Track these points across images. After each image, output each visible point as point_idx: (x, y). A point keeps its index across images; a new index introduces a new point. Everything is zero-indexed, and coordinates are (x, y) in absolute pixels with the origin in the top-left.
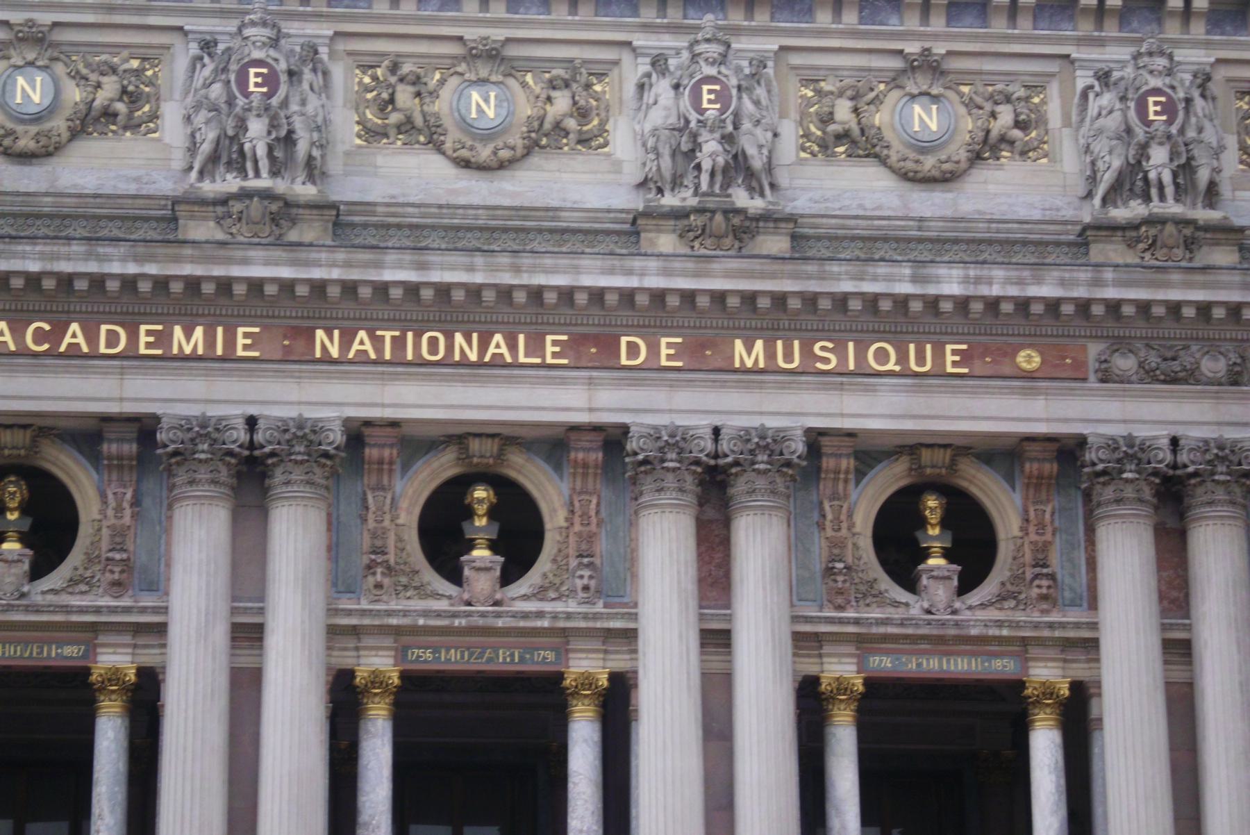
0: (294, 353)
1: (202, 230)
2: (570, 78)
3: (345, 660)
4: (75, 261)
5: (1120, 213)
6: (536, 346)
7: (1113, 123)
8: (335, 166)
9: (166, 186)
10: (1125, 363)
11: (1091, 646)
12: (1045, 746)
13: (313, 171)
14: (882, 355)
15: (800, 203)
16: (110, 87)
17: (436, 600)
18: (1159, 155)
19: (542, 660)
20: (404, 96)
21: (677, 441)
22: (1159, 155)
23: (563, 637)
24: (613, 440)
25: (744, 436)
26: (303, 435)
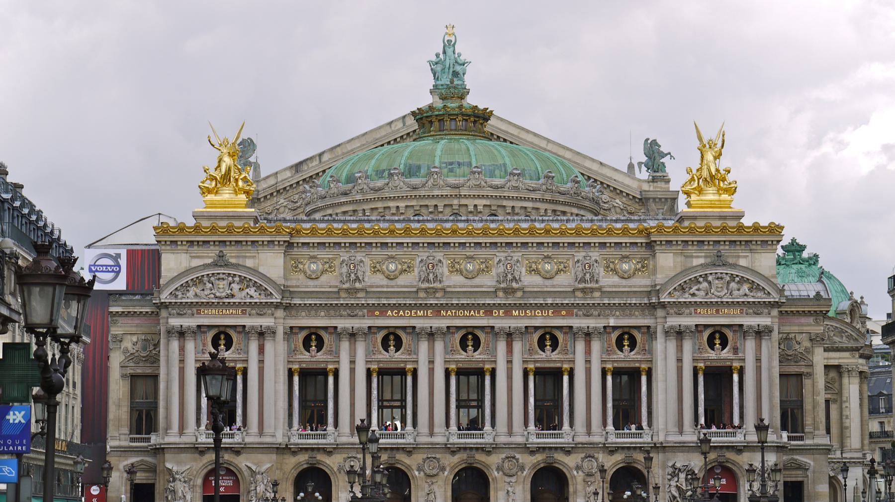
0: (437, 314)
1: (422, 294)
2: (486, 261)
5: (581, 286)
8: (444, 279)
9: (415, 284)
10: (580, 313)
12: (566, 378)
14: (538, 312)
15: (526, 284)
17: (462, 356)
18: (588, 275)
19: (481, 365)
21: (502, 329)
22: (588, 275)
23: (483, 362)
24: (493, 327)
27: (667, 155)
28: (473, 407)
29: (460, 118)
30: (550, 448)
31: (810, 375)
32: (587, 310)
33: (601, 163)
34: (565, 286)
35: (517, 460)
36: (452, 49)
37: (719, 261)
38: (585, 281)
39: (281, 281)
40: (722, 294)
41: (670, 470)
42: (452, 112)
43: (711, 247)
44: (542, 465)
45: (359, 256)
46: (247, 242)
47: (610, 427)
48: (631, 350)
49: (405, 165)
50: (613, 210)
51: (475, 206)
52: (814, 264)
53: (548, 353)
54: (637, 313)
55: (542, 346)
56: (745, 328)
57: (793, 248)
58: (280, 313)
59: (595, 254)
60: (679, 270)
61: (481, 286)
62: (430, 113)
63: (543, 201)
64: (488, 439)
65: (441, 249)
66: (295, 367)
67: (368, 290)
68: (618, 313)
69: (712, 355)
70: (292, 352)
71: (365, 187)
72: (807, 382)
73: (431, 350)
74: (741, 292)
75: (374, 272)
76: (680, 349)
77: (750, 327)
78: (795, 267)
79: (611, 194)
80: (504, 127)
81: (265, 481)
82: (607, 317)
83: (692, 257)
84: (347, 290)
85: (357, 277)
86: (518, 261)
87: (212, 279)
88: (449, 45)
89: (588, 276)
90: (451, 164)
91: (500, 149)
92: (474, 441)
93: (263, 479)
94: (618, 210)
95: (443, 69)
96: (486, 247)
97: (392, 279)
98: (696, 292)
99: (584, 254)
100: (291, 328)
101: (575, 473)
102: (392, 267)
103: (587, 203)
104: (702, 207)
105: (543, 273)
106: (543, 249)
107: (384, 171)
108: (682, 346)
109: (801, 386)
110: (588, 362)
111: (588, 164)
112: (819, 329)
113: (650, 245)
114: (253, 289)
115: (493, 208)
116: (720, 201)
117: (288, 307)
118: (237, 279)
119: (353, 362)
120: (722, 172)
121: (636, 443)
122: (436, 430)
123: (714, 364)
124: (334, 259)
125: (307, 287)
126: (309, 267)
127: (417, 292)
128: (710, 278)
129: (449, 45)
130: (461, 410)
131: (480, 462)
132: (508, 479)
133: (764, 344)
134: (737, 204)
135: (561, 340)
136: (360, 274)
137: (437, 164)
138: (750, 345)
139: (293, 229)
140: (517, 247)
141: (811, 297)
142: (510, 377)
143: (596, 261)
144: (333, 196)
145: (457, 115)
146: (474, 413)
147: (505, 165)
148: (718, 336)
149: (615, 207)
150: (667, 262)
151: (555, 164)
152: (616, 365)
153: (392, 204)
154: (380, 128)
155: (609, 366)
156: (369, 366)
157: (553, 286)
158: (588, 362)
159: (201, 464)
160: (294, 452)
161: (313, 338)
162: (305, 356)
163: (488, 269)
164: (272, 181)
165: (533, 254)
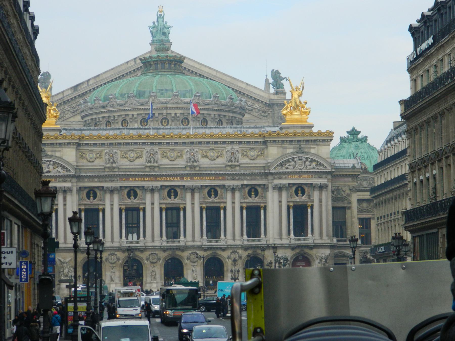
0: (156, 180)
1: (147, 169)
3: (161, 206)
4: (137, 173)
5: (230, 164)
6: (177, 178)
7: (229, 155)
9: (144, 164)
10: (229, 178)
11: (226, 203)
13: (157, 163)
14: (207, 178)
15: (201, 163)
16: (139, 155)
18: (233, 159)
19: (178, 206)
20: (165, 154)
21: (189, 187)
22: (233, 159)
23: (179, 204)
24: (184, 186)
25: (195, 186)
26: (157, 187)
27: (284, 78)
28: (175, 227)
29: (167, 62)
30: (214, 248)
31: (350, 208)
32: (233, 176)
33: (247, 84)
34: (221, 164)
35: (197, 254)
36: (162, 20)
37: (300, 151)
38: (231, 162)
39: (75, 164)
40: (302, 167)
42: (162, 59)
43: (296, 143)
44: (210, 257)
45: (115, 150)
46: (56, 143)
47: (245, 237)
48: (255, 197)
49: (137, 91)
50: (254, 110)
51: (176, 114)
52: (365, 142)
53: (213, 199)
54: (258, 178)
55: (210, 195)
56: (314, 185)
57: (353, 133)
58: (74, 180)
59: (237, 147)
60: (280, 155)
61: (178, 165)
62: (150, 60)
63: (212, 110)
64: (182, 244)
65: (157, 146)
66: (83, 207)
67: (120, 167)
68: (248, 178)
69: (297, 199)
70: (80, 199)
71: (115, 103)
72: (348, 212)
73: (152, 197)
74: (312, 166)
75: (123, 158)
76: (280, 196)
77: (317, 184)
78: (354, 143)
79: (253, 102)
80: (192, 64)
82: (243, 180)
83: (286, 148)
84: (109, 168)
85: (114, 161)
86: (197, 151)
88: (160, 17)
89: (233, 159)
90: (162, 90)
91: (189, 81)
92: (175, 244)
93: (67, 266)
94: (257, 110)
95: (157, 31)
96: (180, 144)
97: (132, 162)
98: (289, 167)
99: (231, 147)
100: (80, 188)
101: (227, 260)
102: (132, 155)
103: (237, 110)
104: (292, 122)
105: (210, 157)
106: (210, 145)
107: (125, 94)
108: (281, 195)
109: (345, 214)
110: (233, 203)
111: (240, 84)
112: (355, 184)
113: (265, 143)
114: (60, 168)
115: (185, 114)
116: (301, 118)
117: (79, 178)
118: (52, 163)
119: (112, 205)
120: (303, 103)
121: (258, 245)
122: (155, 239)
124: (102, 151)
125: (88, 166)
126: (89, 156)
127: (145, 168)
128: (295, 159)
129: (160, 17)
130: (168, 228)
131: (178, 255)
132: (193, 264)
133: (324, 193)
134: (310, 120)
135: (219, 192)
136: (115, 159)
137: (154, 91)
138: (316, 194)
139: (80, 136)
140: (196, 144)
141: (350, 167)
142: (193, 211)
143: (237, 151)
144: (97, 108)
145: (165, 61)
146: (175, 229)
147: (191, 90)
148: (300, 189)
149: (255, 109)
150: (273, 152)
151: (219, 88)
152: (248, 204)
153: (129, 113)
154: (122, 65)
155: (244, 205)
156: (121, 207)
157: (215, 164)
158: (233, 203)
161: (92, 193)
162: (87, 202)
163: (181, 156)
164: (60, 96)
165: (204, 147)
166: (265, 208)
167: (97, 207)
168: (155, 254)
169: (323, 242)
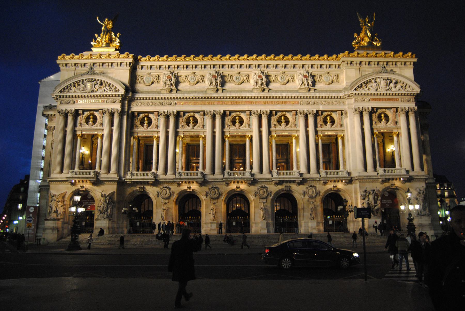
0: (219, 103)
1: (209, 91)
5: (301, 87)
12: (294, 141)
18: (305, 81)
30: (287, 182)
41: (363, 194)
81: (107, 201)
83: (365, 71)
87: (85, 82)
100: (133, 113)
101: (302, 196)
114: (108, 88)
122: (217, 170)
123: (382, 131)
128: (378, 80)
132: (262, 201)
159: (71, 191)
160: (129, 184)
163: (248, 81)
166: (343, 138)
167: (151, 135)
168: (216, 188)
169: (417, 174)
